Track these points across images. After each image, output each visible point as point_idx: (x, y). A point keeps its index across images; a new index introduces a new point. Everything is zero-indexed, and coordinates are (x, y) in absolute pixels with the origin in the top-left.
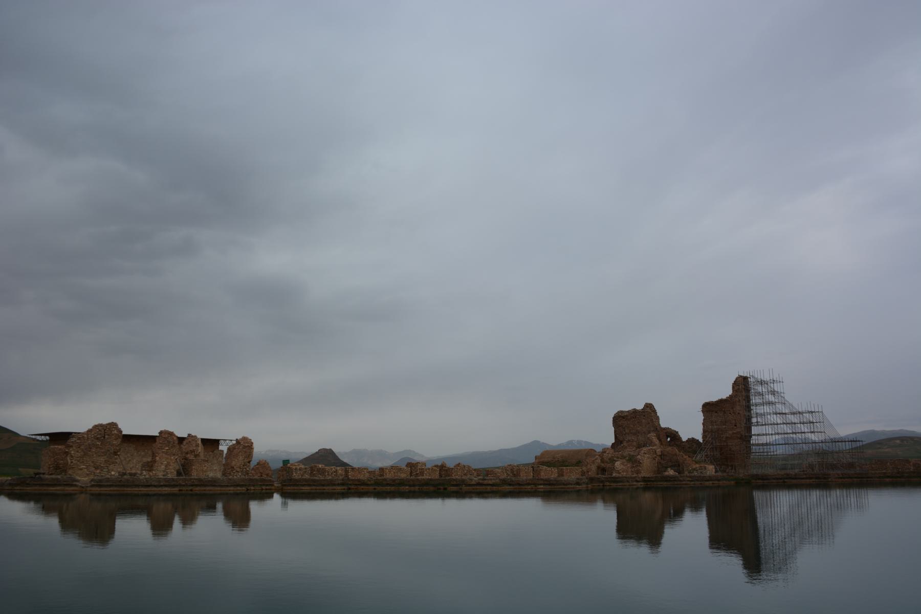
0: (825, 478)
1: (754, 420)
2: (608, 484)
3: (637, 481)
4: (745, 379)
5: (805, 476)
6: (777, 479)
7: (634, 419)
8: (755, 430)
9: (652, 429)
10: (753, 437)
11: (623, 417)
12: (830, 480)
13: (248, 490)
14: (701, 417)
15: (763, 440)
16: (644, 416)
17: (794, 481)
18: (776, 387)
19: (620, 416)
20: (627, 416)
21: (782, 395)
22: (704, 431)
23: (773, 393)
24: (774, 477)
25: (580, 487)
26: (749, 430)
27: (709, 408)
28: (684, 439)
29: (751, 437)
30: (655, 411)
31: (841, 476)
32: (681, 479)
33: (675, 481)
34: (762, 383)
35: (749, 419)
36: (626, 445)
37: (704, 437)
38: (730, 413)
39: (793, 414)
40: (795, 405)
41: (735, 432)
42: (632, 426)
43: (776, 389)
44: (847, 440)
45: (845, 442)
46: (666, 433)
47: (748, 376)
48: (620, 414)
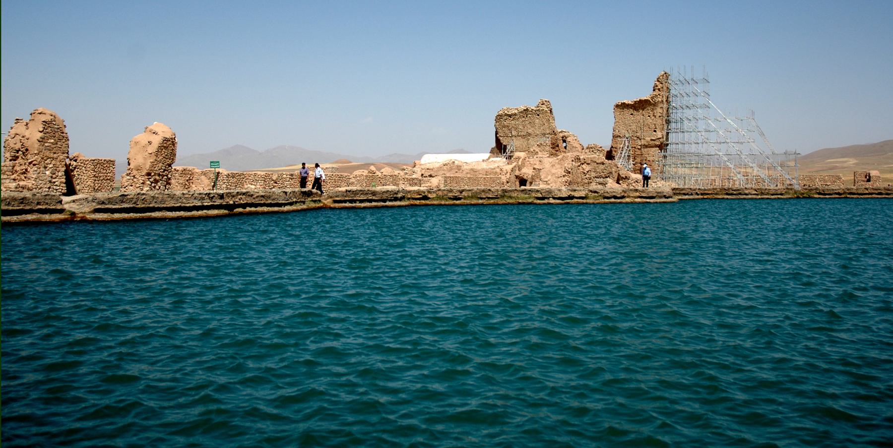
7: (524, 119)
8: (672, 138)
9: (548, 132)
11: (510, 116)
16: (538, 115)
19: (506, 115)
20: (515, 114)
32: (747, 192)
33: (740, 194)
36: (537, 150)
38: (649, 116)
41: (653, 138)
42: (521, 127)
46: (563, 137)
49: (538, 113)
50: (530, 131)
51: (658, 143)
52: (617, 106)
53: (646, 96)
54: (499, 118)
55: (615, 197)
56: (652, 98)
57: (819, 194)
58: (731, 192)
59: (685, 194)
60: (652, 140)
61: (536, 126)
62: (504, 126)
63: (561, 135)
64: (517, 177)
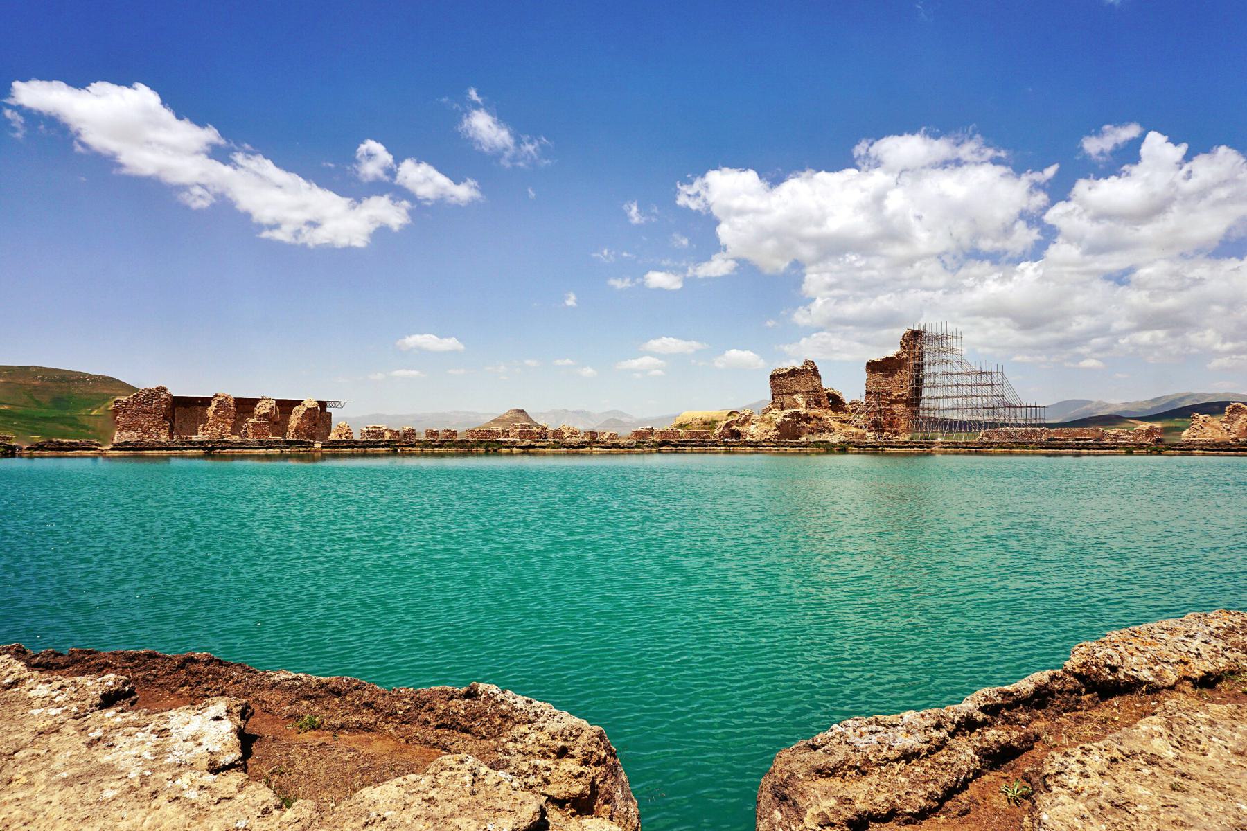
0: (928, 447)
1: (926, 381)
3: (717, 446)
4: (916, 334)
8: (926, 392)
9: (811, 389)
11: (781, 376)
12: (933, 449)
13: (282, 452)
14: (864, 376)
15: (932, 403)
18: (954, 343)
19: (778, 375)
20: (785, 374)
21: (959, 352)
22: (868, 393)
26: (917, 391)
27: (873, 367)
28: (847, 401)
29: (920, 400)
30: (815, 370)
33: (758, 446)
34: (932, 339)
35: (918, 380)
37: (867, 398)
40: (973, 366)
43: (955, 347)
45: (1030, 407)
47: (922, 329)
49: (802, 372)
50: (797, 389)
51: (904, 398)
53: (892, 352)
54: (772, 377)
55: (573, 447)
56: (898, 355)
57: (855, 447)
59: (695, 446)
60: (899, 396)
61: (803, 383)
62: (777, 385)
63: (826, 392)
64: (733, 431)
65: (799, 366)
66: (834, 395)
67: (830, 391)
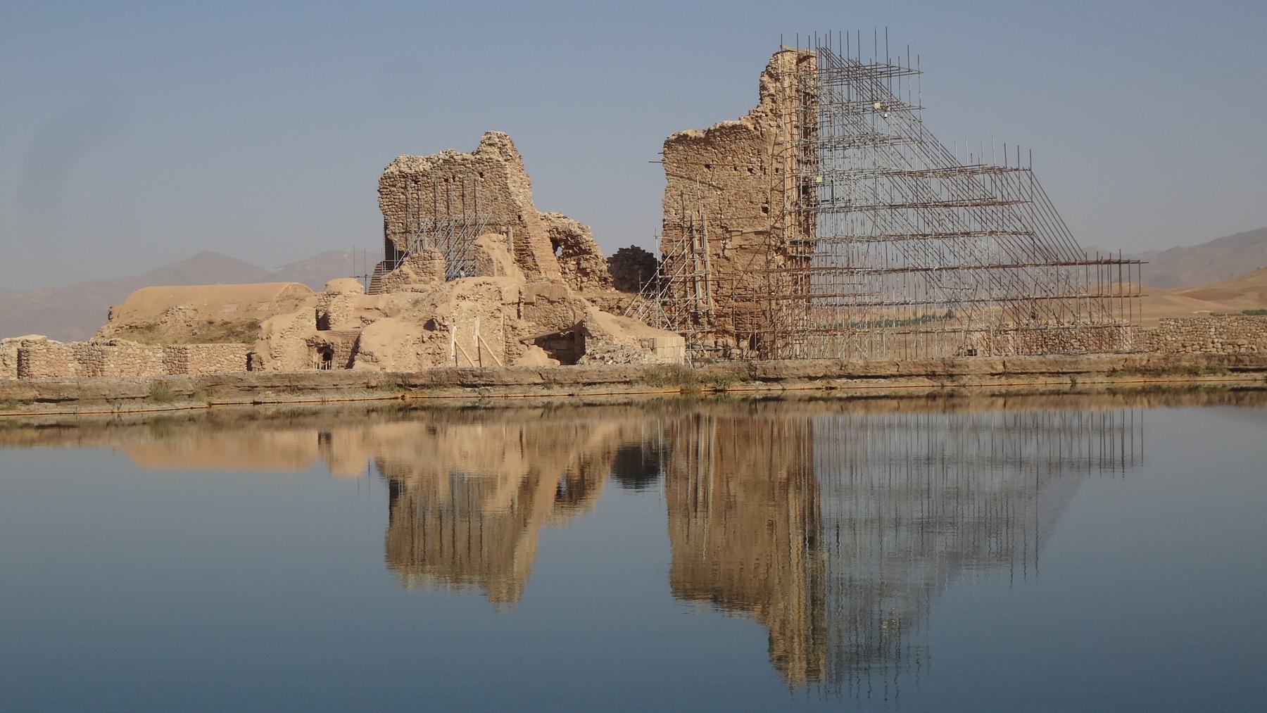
1: (821, 194)
2: (271, 396)
5: (894, 371)
6: (811, 378)
8: (825, 226)
9: (505, 218)
10: (821, 248)
12: (965, 380)
17: (861, 387)
18: (901, 88)
19: (404, 176)
23: (894, 106)
24: (801, 373)
25: (166, 406)
26: (806, 221)
31: (1000, 368)
32: (509, 379)
39: (947, 173)
44: (1092, 258)
48: (405, 169)
52: (668, 144)
54: (388, 184)
58: (471, 379)
65: (463, 152)
66: (570, 234)
67: (558, 223)
